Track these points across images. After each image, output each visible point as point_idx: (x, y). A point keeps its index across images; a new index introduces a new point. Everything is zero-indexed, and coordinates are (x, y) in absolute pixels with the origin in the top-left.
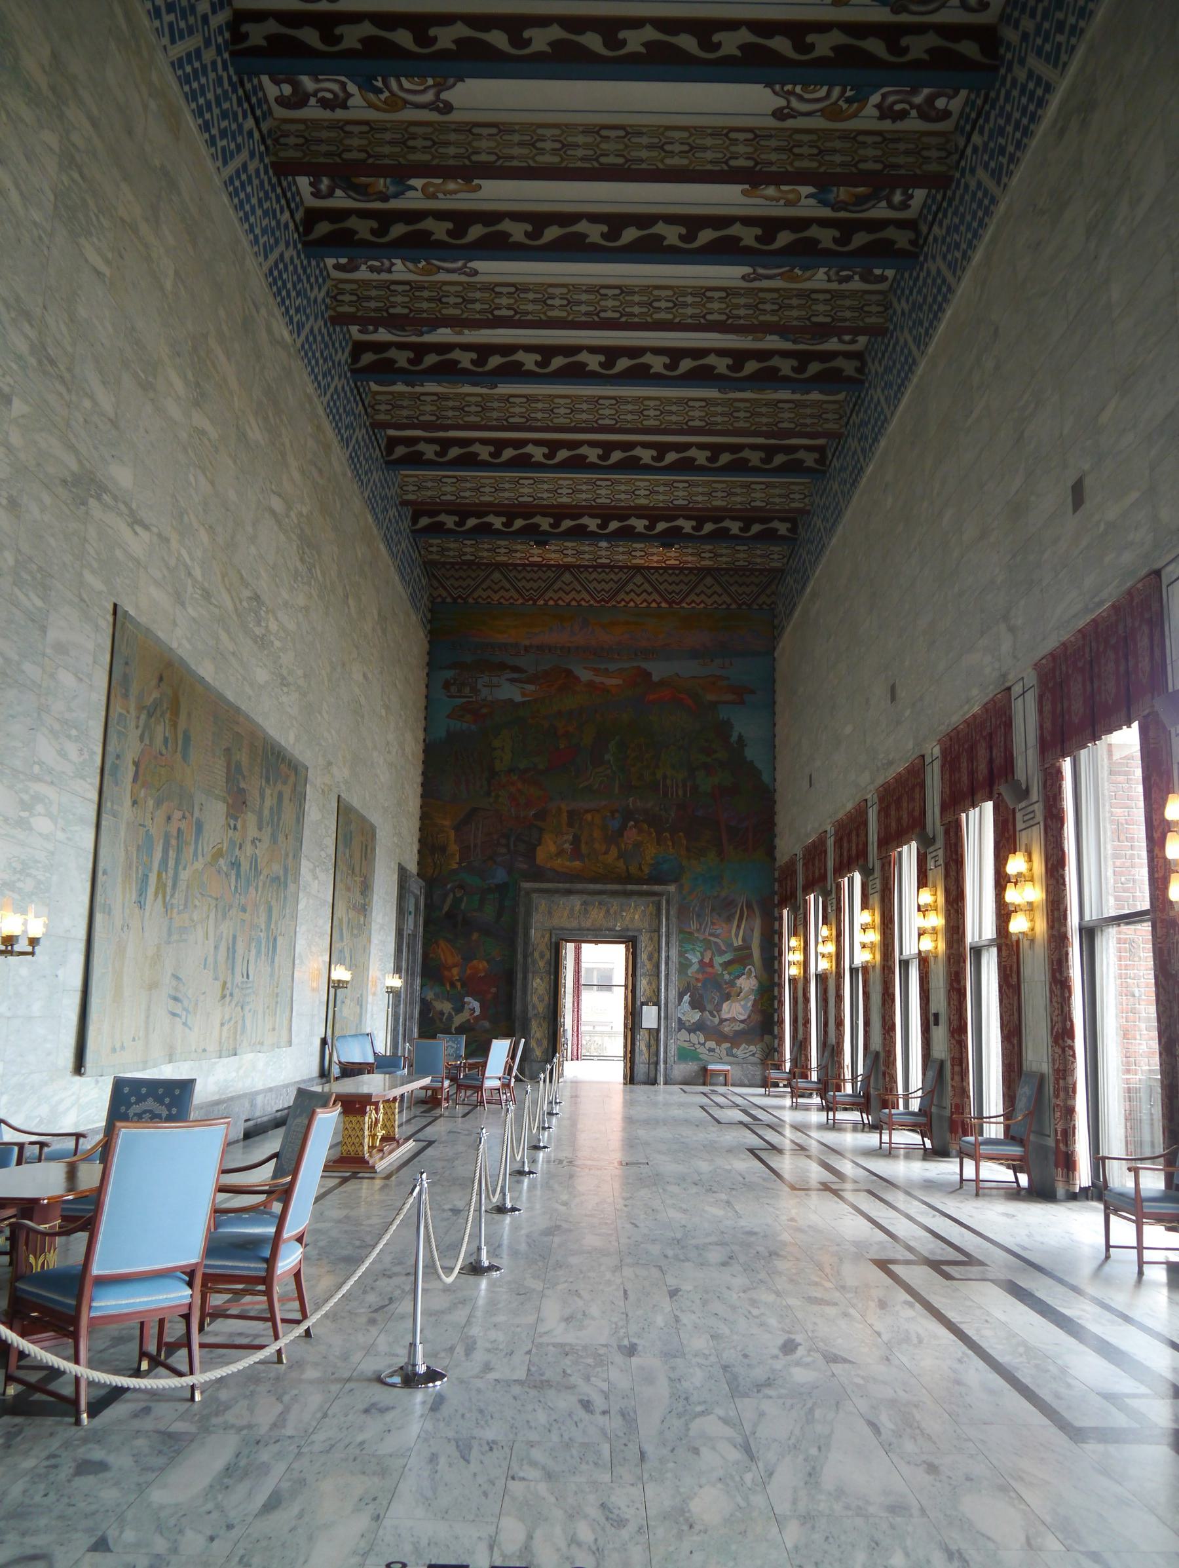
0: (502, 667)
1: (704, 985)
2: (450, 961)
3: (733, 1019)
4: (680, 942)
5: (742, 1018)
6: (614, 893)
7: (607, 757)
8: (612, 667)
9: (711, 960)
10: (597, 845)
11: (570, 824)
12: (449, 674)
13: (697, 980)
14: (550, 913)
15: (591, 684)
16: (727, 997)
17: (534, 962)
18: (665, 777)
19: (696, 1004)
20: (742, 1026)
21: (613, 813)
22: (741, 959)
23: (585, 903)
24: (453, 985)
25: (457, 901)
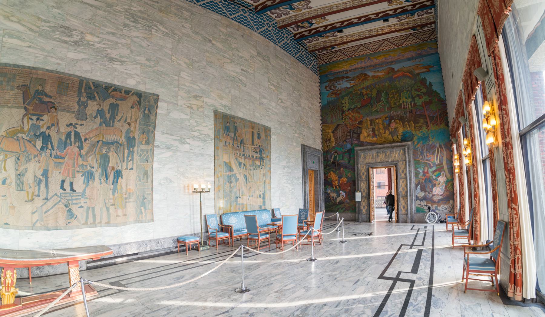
0: (343, 78)
1: (425, 181)
2: (335, 179)
3: (438, 195)
4: (415, 164)
5: (441, 194)
6: (388, 147)
7: (382, 99)
8: (380, 69)
9: (427, 171)
10: (381, 131)
11: (371, 125)
12: (327, 84)
13: (422, 179)
14: (365, 158)
15: (373, 76)
16: (435, 185)
17: (361, 177)
18: (403, 102)
19: (423, 189)
20: (441, 197)
21: (386, 118)
22: (440, 169)
23: (377, 153)
24: (336, 187)
25: (335, 157)
